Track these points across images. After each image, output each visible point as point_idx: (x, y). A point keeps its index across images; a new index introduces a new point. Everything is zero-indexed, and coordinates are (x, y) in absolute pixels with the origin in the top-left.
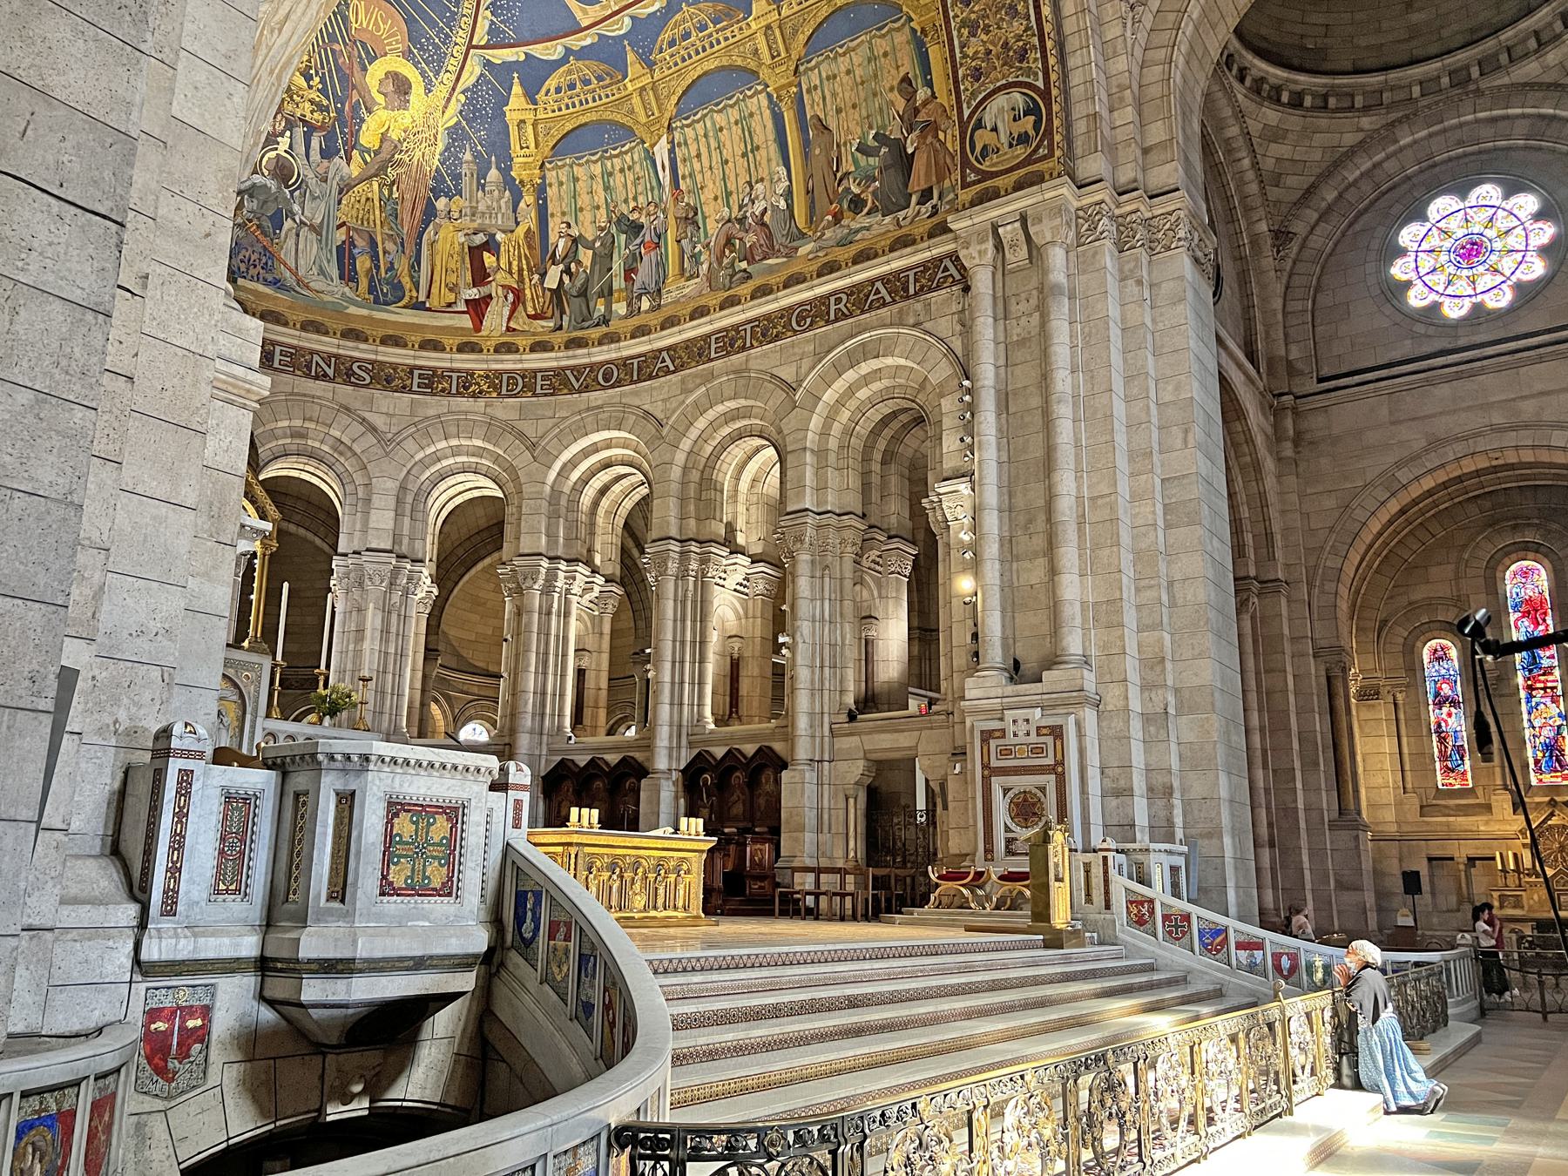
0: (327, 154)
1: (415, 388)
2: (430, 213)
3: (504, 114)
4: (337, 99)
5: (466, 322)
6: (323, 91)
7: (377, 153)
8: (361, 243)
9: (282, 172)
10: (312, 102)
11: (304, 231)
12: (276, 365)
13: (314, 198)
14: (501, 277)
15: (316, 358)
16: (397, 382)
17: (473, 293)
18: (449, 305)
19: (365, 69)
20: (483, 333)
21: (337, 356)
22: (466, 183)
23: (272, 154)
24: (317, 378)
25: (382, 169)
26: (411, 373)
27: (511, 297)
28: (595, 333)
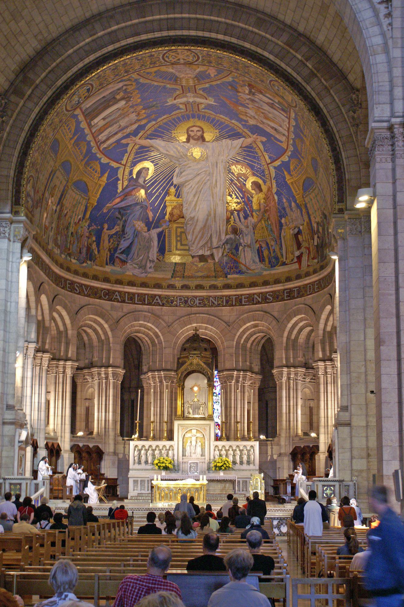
0: (246, 217)
1: (285, 298)
2: (281, 225)
3: (286, 182)
4: (242, 198)
5: (296, 266)
6: (237, 198)
7: (260, 210)
8: (264, 245)
9: (235, 231)
10: (235, 203)
11: (246, 248)
12: (243, 303)
13: (246, 235)
14: (304, 244)
15: (255, 296)
16: (280, 297)
17: (297, 253)
18: (292, 260)
19: (245, 185)
20: (302, 269)
21: (262, 293)
22: (288, 210)
23: (230, 226)
24: (256, 304)
25: (263, 215)
26: (284, 292)
27: (307, 251)
28: (324, 262)
